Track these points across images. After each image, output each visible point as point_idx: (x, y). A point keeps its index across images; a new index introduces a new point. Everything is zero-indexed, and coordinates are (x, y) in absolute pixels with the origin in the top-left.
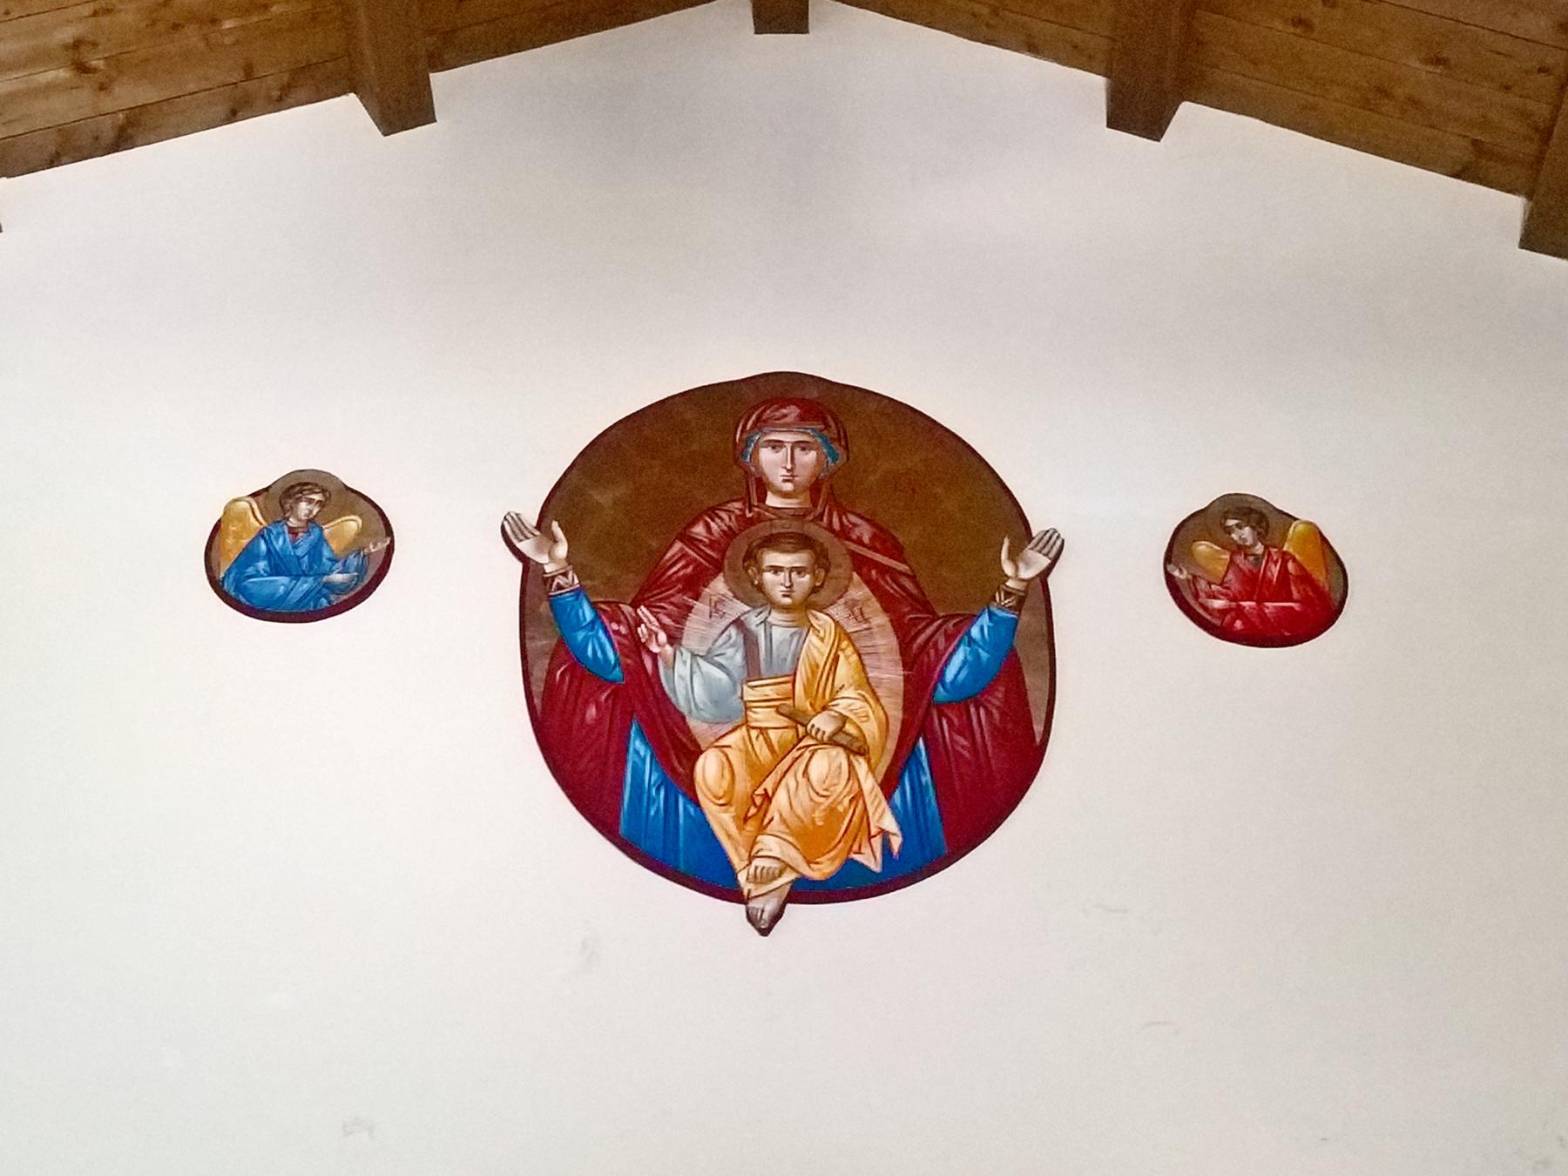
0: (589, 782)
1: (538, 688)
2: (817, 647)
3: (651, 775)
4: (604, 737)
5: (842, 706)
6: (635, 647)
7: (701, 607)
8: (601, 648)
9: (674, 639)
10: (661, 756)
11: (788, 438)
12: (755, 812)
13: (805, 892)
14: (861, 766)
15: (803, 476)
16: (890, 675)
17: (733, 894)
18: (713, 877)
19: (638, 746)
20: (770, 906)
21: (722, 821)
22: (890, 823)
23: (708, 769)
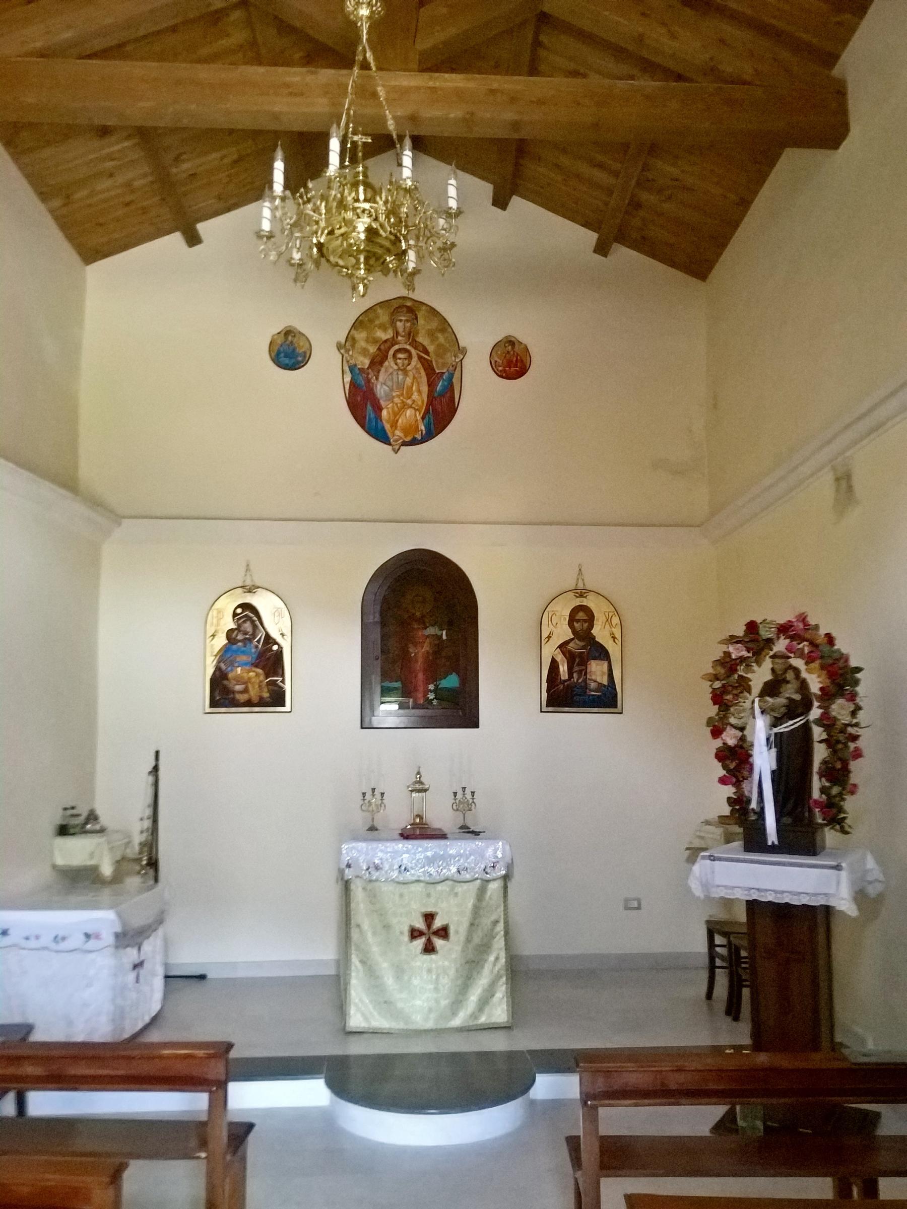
0: (360, 420)
1: (347, 392)
2: (409, 380)
3: (372, 415)
4: (362, 403)
5: (413, 397)
6: (368, 381)
7: (383, 370)
8: (361, 381)
9: (377, 379)
10: (375, 411)
11: (403, 318)
12: (394, 425)
13: (405, 444)
14: (417, 413)
15: (407, 330)
16: (425, 389)
17: (390, 444)
19: (369, 407)
20: (397, 447)
21: (387, 427)
22: (423, 428)
23: (384, 413)
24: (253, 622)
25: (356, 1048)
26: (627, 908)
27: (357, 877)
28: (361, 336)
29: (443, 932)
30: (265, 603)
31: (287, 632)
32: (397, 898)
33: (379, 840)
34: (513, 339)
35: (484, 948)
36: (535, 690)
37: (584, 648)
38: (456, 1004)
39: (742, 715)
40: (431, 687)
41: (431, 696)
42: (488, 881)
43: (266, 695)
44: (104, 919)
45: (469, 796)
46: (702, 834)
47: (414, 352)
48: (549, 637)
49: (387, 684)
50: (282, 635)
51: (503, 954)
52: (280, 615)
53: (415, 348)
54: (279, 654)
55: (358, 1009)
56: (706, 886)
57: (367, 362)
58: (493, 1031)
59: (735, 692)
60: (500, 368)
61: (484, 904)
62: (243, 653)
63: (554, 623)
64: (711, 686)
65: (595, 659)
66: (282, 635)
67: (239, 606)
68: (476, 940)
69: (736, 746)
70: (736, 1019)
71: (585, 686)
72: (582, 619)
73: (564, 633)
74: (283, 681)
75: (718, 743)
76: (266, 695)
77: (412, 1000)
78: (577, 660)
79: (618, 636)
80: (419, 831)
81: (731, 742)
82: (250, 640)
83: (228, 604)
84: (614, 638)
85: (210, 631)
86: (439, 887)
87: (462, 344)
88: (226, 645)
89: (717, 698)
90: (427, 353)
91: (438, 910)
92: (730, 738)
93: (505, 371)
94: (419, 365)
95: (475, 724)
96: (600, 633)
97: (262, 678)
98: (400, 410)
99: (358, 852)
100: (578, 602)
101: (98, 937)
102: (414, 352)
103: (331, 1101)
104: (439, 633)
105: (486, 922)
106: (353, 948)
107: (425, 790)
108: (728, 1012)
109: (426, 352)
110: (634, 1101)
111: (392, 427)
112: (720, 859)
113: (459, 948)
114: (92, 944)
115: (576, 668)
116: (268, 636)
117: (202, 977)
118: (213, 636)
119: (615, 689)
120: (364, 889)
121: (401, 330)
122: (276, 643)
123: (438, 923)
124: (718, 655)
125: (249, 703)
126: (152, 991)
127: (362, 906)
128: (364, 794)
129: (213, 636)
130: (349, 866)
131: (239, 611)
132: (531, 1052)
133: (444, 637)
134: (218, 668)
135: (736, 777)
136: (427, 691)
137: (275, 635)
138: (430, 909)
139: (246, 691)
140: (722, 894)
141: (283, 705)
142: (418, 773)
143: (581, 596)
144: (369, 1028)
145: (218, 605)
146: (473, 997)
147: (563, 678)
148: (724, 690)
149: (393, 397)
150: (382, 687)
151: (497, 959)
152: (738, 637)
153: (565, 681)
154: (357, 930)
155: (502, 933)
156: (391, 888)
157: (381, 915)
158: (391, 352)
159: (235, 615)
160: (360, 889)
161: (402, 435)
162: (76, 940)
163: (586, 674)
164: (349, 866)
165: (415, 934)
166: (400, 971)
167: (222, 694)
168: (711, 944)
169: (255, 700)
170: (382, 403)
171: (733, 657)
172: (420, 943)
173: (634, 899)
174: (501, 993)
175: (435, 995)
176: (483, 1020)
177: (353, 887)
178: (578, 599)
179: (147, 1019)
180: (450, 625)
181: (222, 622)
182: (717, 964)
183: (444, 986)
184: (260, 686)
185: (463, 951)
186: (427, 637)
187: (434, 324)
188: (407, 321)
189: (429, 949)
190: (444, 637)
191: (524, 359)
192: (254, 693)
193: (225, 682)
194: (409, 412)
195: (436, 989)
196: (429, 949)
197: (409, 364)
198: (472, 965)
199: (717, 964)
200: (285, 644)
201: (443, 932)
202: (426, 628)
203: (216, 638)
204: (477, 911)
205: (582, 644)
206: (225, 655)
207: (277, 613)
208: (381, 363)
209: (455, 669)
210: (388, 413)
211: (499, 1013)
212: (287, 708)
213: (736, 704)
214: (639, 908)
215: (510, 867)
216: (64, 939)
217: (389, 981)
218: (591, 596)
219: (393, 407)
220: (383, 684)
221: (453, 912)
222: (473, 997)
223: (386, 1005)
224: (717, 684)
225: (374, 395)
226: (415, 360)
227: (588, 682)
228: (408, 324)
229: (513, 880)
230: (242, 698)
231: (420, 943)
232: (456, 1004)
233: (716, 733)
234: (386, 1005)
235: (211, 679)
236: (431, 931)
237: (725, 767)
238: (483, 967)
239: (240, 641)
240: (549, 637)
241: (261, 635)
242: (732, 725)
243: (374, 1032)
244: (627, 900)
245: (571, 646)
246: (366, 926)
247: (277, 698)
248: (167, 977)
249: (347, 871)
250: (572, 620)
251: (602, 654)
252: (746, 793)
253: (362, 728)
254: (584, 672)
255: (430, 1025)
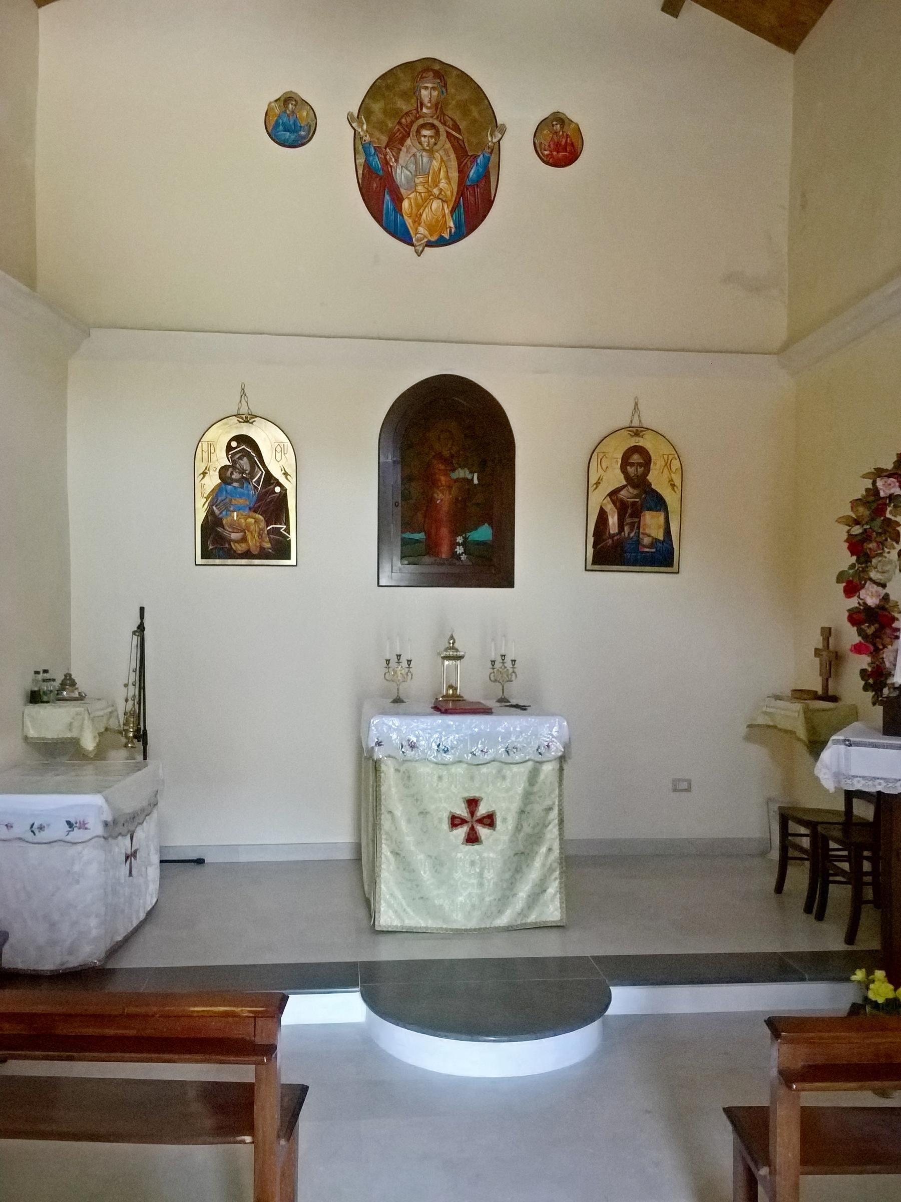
0: (377, 213)
1: (360, 176)
2: (436, 164)
3: (391, 206)
4: (379, 191)
5: (441, 185)
6: (387, 163)
7: (404, 149)
8: (376, 162)
9: (397, 161)
10: (393, 200)
11: (430, 85)
12: (417, 220)
13: (430, 244)
14: (446, 207)
15: (433, 100)
16: (454, 175)
17: (412, 245)
18: (404, 236)
19: (387, 197)
20: (421, 249)
21: (409, 222)
22: (452, 225)
23: (406, 204)
24: (250, 458)
25: (387, 952)
26: (675, 790)
27: (389, 756)
28: (377, 107)
29: (489, 821)
30: (266, 437)
31: (291, 471)
32: (435, 778)
33: (406, 714)
34: (562, 117)
35: (536, 839)
36: (577, 544)
37: (638, 496)
38: (503, 901)
39: (887, 568)
40: (460, 539)
41: (459, 550)
42: (541, 763)
43: (267, 545)
44: (90, 805)
45: (509, 664)
46: (768, 710)
47: (442, 128)
48: (597, 484)
49: (408, 535)
50: (286, 474)
51: (556, 846)
52: (283, 451)
53: (444, 124)
54: (283, 498)
55: (390, 906)
56: (837, 775)
57: (384, 139)
58: (546, 930)
59: (879, 539)
60: (546, 153)
61: (536, 789)
62: (242, 495)
63: (604, 467)
64: (848, 532)
65: (650, 509)
66: (286, 474)
67: (233, 439)
68: (527, 829)
69: (878, 607)
70: (820, 917)
71: (638, 542)
72: (636, 461)
73: (615, 478)
74: (288, 530)
75: (853, 602)
76: (267, 545)
77: (447, 896)
78: (629, 511)
79: (678, 482)
80: (450, 705)
81: (872, 601)
82: (248, 480)
83: (221, 436)
84: (673, 486)
85: (200, 468)
86: (484, 770)
87: (500, 121)
88: (219, 485)
89: (856, 546)
90: (458, 130)
91: (483, 795)
92: (870, 597)
93: (551, 155)
94: (448, 145)
95: (511, 585)
96: (657, 480)
97: (262, 524)
98: (425, 200)
99: (391, 729)
100: (634, 442)
101: (83, 826)
102: (442, 128)
103: (368, 1017)
104: (469, 477)
105: (538, 808)
106: (384, 837)
107: (460, 658)
108: (808, 909)
109: (457, 128)
110: (860, 1084)
111: (414, 222)
112: (857, 744)
113: (506, 838)
114: (77, 835)
115: (628, 520)
116: (269, 476)
117: (200, 862)
118: (204, 473)
119: (672, 545)
120: (397, 770)
121: (426, 100)
122: (279, 484)
123: (482, 810)
124: (860, 493)
125: (248, 555)
126: (146, 883)
127: (394, 790)
128: (388, 661)
129: (204, 473)
130: (379, 744)
131: (234, 444)
132: (597, 959)
133: (476, 481)
134: (210, 512)
135: (874, 645)
136: (454, 544)
137: (277, 473)
138: (473, 794)
139: (244, 540)
140: (879, 788)
141: (289, 558)
142: (452, 637)
143: (637, 434)
144: (402, 927)
145: (209, 436)
146: (523, 892)
147: (612, 532)
148: (866, 537)
149: (416, 185)
150: (403, 539)
151: (550, 850)
152: (887, 470)
153: (614, 535)
154: (389, 816)
155: (556, 821)
156: (428, 770)
157: (417, 800)
158: (415, 127)
159: (229, 448)
160: (392, 770)
161: (426, 233)
162: (58, 830)
163: (639, 528)
164: (379, 744)
165: (455, 821)
166: (438, 863)
167: (216, 543)
168: (784, 832)
169: (255, 551)
170: (403, 191)
171: (882, 494)
172: (462, 832)
173: (685, 780)
174: (553, 888)
175: (479, 891)
176: (532, 918)
177: (383, 767)
178: (634, 439)
179: (142, 916)
180: (481, 467)
181: (214, 457)
182: (790, 855)
183: (489, 881)
184: (260, 535)
185: (511, 841)
186: (456, 480)
187: (465, 95)
188: (433, 88)
189: (472, 839)
190: (476, 481)
191: (576, 144)
192: (253, 543)
193: (219, 529)
194: (436, 204)
195: (481, 885)
196: (472, 839)
197: (435, 144)
198: (520, 858)
199: (790, 855)
200: (290, 486)
201: (489, 821)
202: (454, 470)
203: (207, 476)
204: (528, 796)
205: (636, 492)
206: (216, 498)
207: (279, 449)
208: (402, 141)
209: (487, 518)
210: (411, 204)
211: (552, 910)
212: (292, 561)
213: (881, 555)
214: (688, 790)
215: (567, 746)
216: (41, 828)
217: (426, 874)
218: (648, 436)
219: (416, 199)
220: (404, 535)
221: (500, 799)
222: (523, 892)
223: (421, 900)
224: (857, 530)
225: (393, 181)
226: (443, 137)
227: (641, 536)
228: (435, 93)
229: (569, 762)
230: (240, 548)
231: (462, 832)
232: (503, 901)
233: (851, 589)
234: (421, 900)
235: (202, 526)
236: (475, 818)
237: (860, 632)
238: (533, 860)
239: (236, 481)
240: (597, 484)
241: (260, 474)
242: (874, 582)
243: (410, 932)
244: (676, 782)
245: (623, 494)
246: (398, 813)
247: (281, 550)
248: (161, 862)
249: (376, 749)
250: (625, 462)
251: (659, 503)
252: (888, 665)
253: (379, 586)
254: (636, 526)
255: (473, 924)
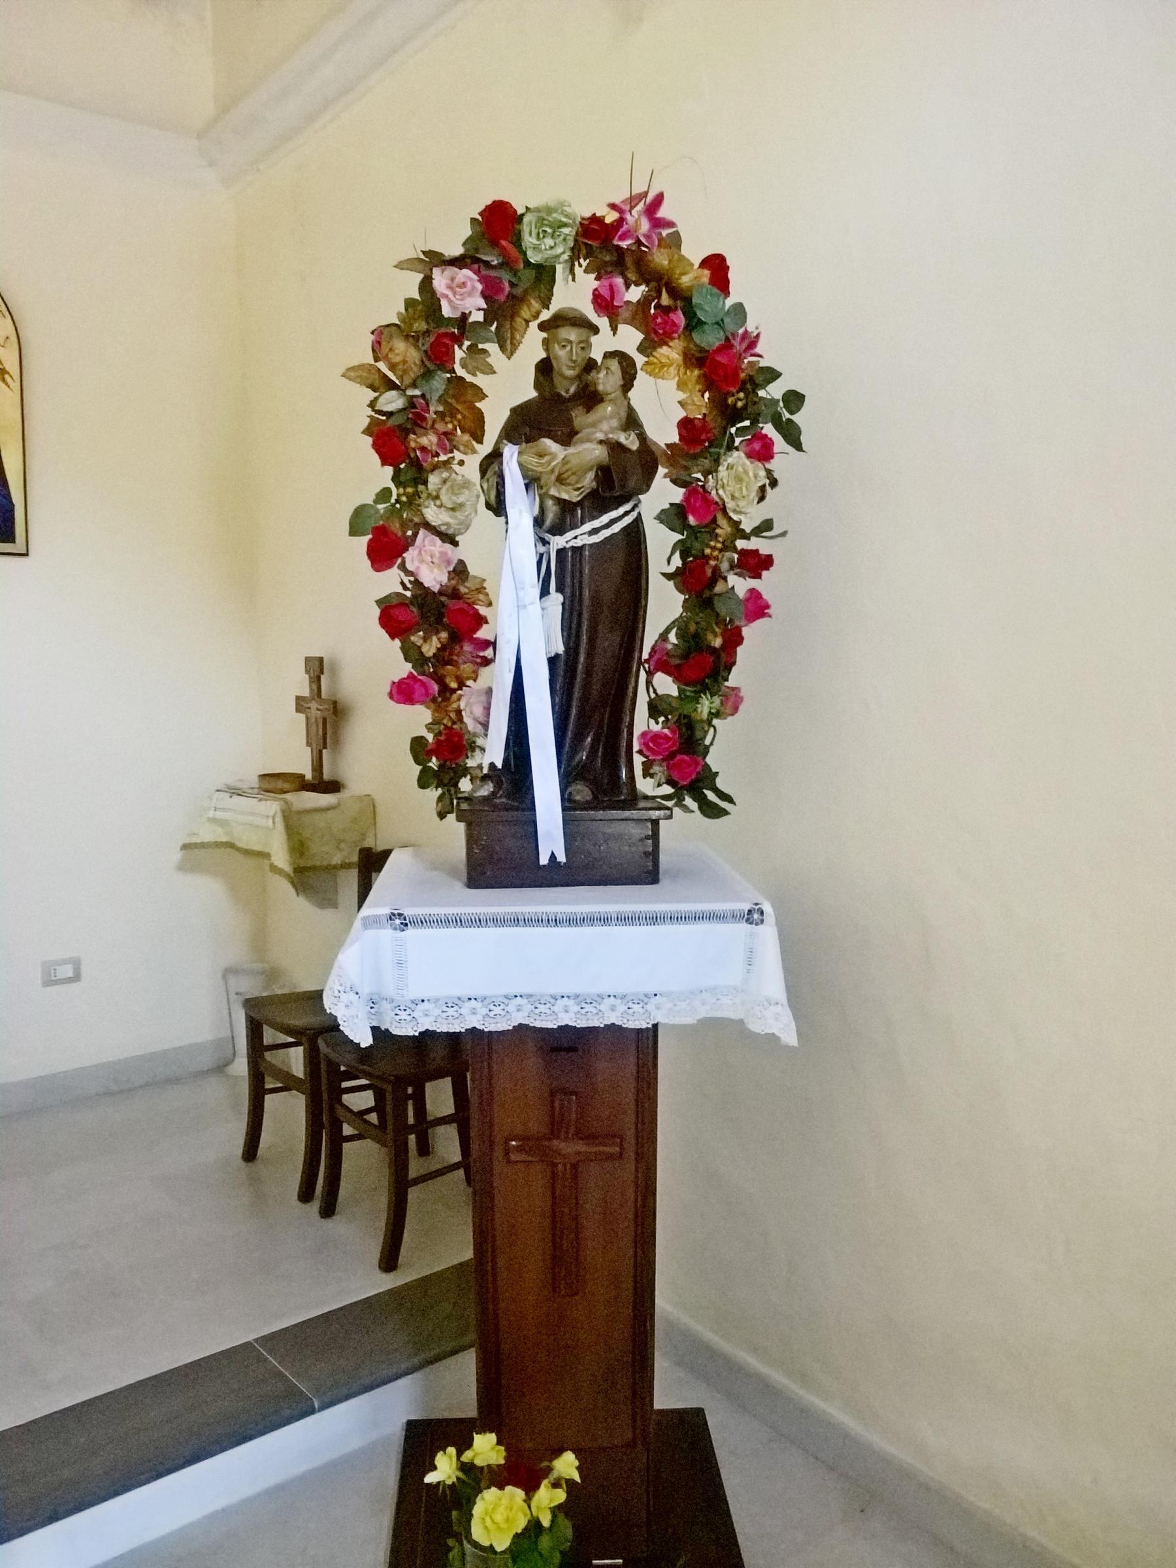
59: (440, 427)
64: (372, 405)
75: (390, 582)
81: (434, 578)
89: (389, 440)
92: (428, 565)
108: (306, 1195)
112: (422, 922)
124: (392, 313)
135: (441, 681)
171: (446, 311)
173: (65, 962)
199: (268, 1086)
214: (76, 977)
224: (392, 401)
233: (385, 549)
237: (411, 653)
252: (470, 723)
